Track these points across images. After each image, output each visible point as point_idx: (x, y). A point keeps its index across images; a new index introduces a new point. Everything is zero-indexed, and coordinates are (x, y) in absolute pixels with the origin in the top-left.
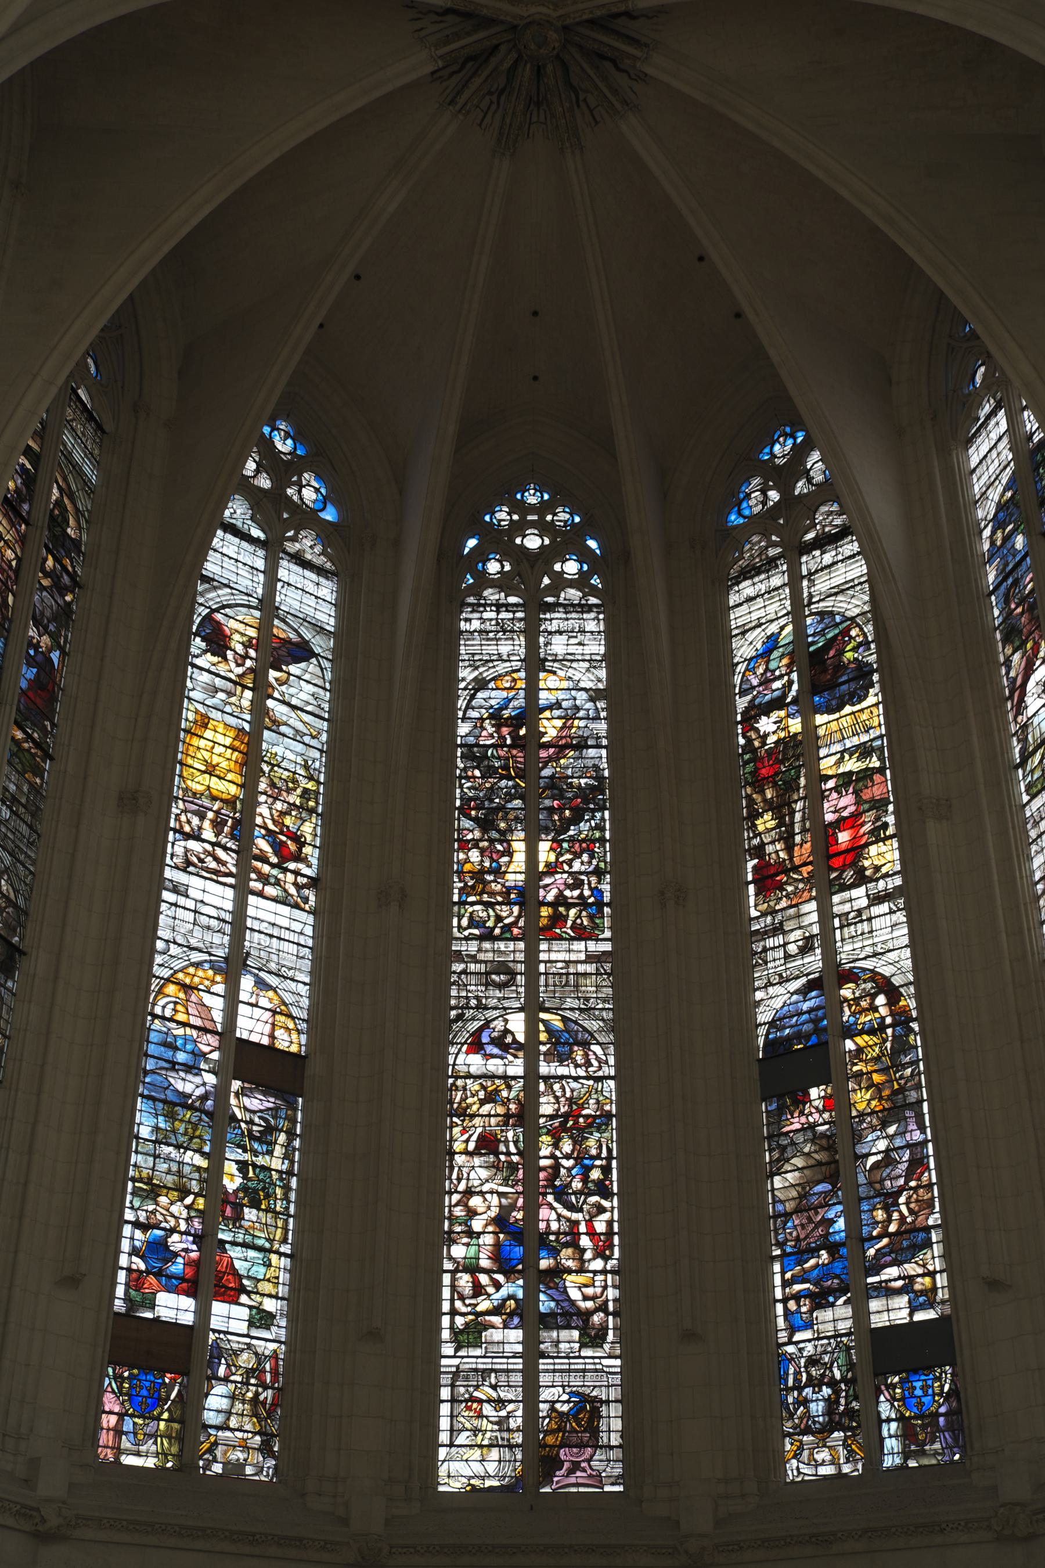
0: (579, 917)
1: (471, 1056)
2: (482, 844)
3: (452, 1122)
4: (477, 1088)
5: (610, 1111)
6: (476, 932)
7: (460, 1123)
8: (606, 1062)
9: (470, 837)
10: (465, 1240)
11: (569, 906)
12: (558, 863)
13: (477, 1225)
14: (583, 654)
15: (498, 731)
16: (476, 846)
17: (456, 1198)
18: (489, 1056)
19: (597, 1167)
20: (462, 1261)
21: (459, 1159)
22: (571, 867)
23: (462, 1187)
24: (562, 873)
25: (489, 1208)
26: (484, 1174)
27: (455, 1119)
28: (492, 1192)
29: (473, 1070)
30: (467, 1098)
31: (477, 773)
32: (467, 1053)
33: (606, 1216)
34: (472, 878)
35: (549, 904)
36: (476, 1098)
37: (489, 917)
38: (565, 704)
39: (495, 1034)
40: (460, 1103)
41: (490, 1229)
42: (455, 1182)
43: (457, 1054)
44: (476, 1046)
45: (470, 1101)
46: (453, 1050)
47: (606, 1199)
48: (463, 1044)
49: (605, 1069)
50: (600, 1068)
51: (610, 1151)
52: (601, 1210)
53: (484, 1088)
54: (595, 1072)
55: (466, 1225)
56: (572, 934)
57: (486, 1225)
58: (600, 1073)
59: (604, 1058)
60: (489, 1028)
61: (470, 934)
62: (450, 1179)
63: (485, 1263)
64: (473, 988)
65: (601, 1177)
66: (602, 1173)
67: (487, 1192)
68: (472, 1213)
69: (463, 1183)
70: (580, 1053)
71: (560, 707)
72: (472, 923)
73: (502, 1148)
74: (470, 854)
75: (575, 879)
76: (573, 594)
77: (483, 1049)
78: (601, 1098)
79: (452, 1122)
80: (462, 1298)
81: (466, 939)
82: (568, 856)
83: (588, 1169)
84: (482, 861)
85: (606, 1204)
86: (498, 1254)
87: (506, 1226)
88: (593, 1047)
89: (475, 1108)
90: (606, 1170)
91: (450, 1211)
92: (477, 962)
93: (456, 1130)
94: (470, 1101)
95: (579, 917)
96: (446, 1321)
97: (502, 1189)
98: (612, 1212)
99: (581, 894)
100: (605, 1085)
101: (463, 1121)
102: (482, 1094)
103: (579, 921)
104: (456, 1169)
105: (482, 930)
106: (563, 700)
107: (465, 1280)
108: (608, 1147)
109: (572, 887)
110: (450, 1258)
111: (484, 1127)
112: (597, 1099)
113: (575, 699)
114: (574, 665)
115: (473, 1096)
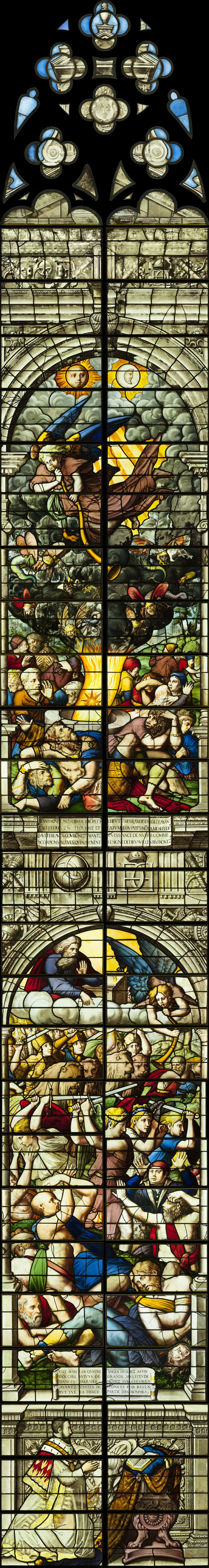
0: (164, 778)
1: (32, 994)
2: (41, 659)
3: (8, 1089)
4: (41, 1041)
5: (200, 1074)
6: (34, 802)
7: (19, 1090)
8: (196, 1003)
9: (23, 648)
10: (30, 1252)
11: (150, 763)
12: (134, 692)
13: (44, 1230)
14: (174, 324)
15: (61, 466)
16: (32, 663)
17: (16, 1194)
18: (56, 995)
19: (182, 1150)
20: (25, 1279)
21: (19, 1142)
22: (152, 696)
23: (23, 1180)
24: (140, 708)
25: (59, 1208)
26: (51, 1161)
27: (12, 1085)
28: (63, 1186)
29: (35, 1014)
30: (28, 1056)
31: (31, 540)
32: (28, 989)
33: (192, 1218)
34: (28, 718)
35: (122, 759)
36: (39, 1056)
37: (52, 779)
38: (146, 416)
39: (63, 962)
40: (19, 1063)
41: (60, 1236)
42: (15, 1173)
43: (14, 992)
44: (38, 979)
45: (32, 1059)
46: (7, 985)
47: (192, 1194)
48: (21, 977)
49: (195, 1011)
50: (188, 1010)
51: (197, 1129)
52: (187, 1209)
53: (49, 1040)
54: (181, 1016)
55: (29, 1231)
56: (155, 806)
57: (56, 1231)
58: (188, 1019)
59: (193, 995)
60: (54, 952)
61: (26, 806)
62: (8, 1169)
63: (55, 1281)
64: (33, 891)
65: (187, 1164)
66: (189, 1158)
67: (56, 1187)
68: (38, 1215)
69: (26, 1174)
70: (162, 989)
71: (139, 423)
72: (30, 790)
73: (74, 1128)
74: (24, 676)
75: (159, 719)
76: (158, 202)
77: (48, 984)
78: (188, 1056)
79: (8, 1089)
80: (27, 1327)
81: (21, 813)
82: (149, 681)
83: (170, 1153)
84: (41, 688)
85: (193, 1201)
86: (70, 1271)
87: (80, 1232)
88: (179, 981)
89: (39, 1069)
90: (193, 1154)
91: (9, 1212)
92: (38, 851)
93: (15, 1100)
94: (32, 1059)
95: (164, 778)
96: (7, 1356)
97: (75, 1182)
98: (200, 1212)
99: (167, 747)
100: (194, 1036)
101: (23, 1088)
102: (47, 1051)
103: (163, 786)
104: (16, 1155)
105: (43, 799)
106: (145, 408)
107: (29, 1302)
108: (194, 1123)
109: (155, 732)
110: (11, 1275)
111: (51, 1095)
112: (183, 1057)
113: (161, 406)
114: (161, 343)
115: (36, 1052)
